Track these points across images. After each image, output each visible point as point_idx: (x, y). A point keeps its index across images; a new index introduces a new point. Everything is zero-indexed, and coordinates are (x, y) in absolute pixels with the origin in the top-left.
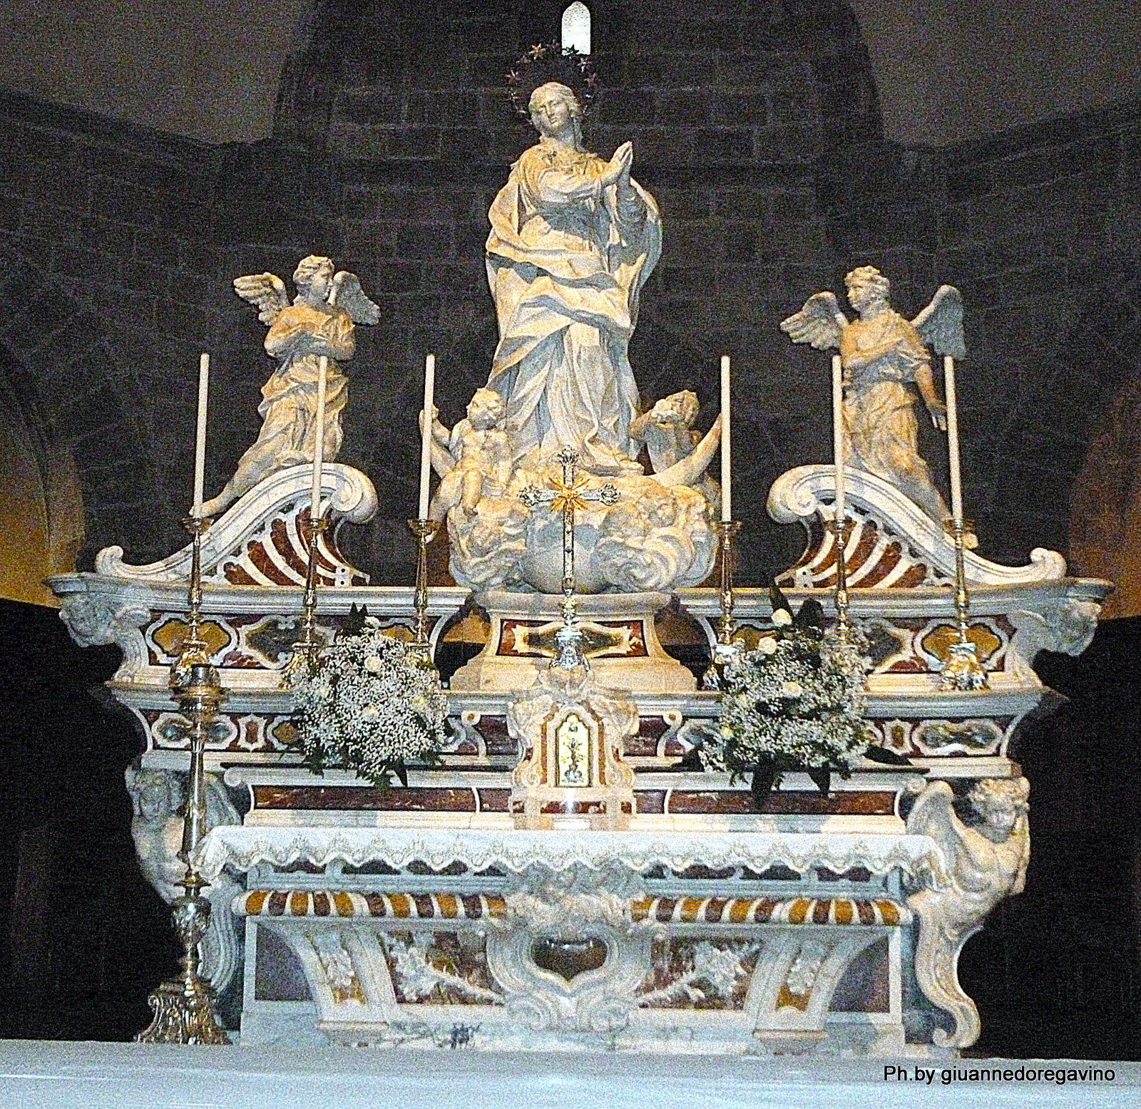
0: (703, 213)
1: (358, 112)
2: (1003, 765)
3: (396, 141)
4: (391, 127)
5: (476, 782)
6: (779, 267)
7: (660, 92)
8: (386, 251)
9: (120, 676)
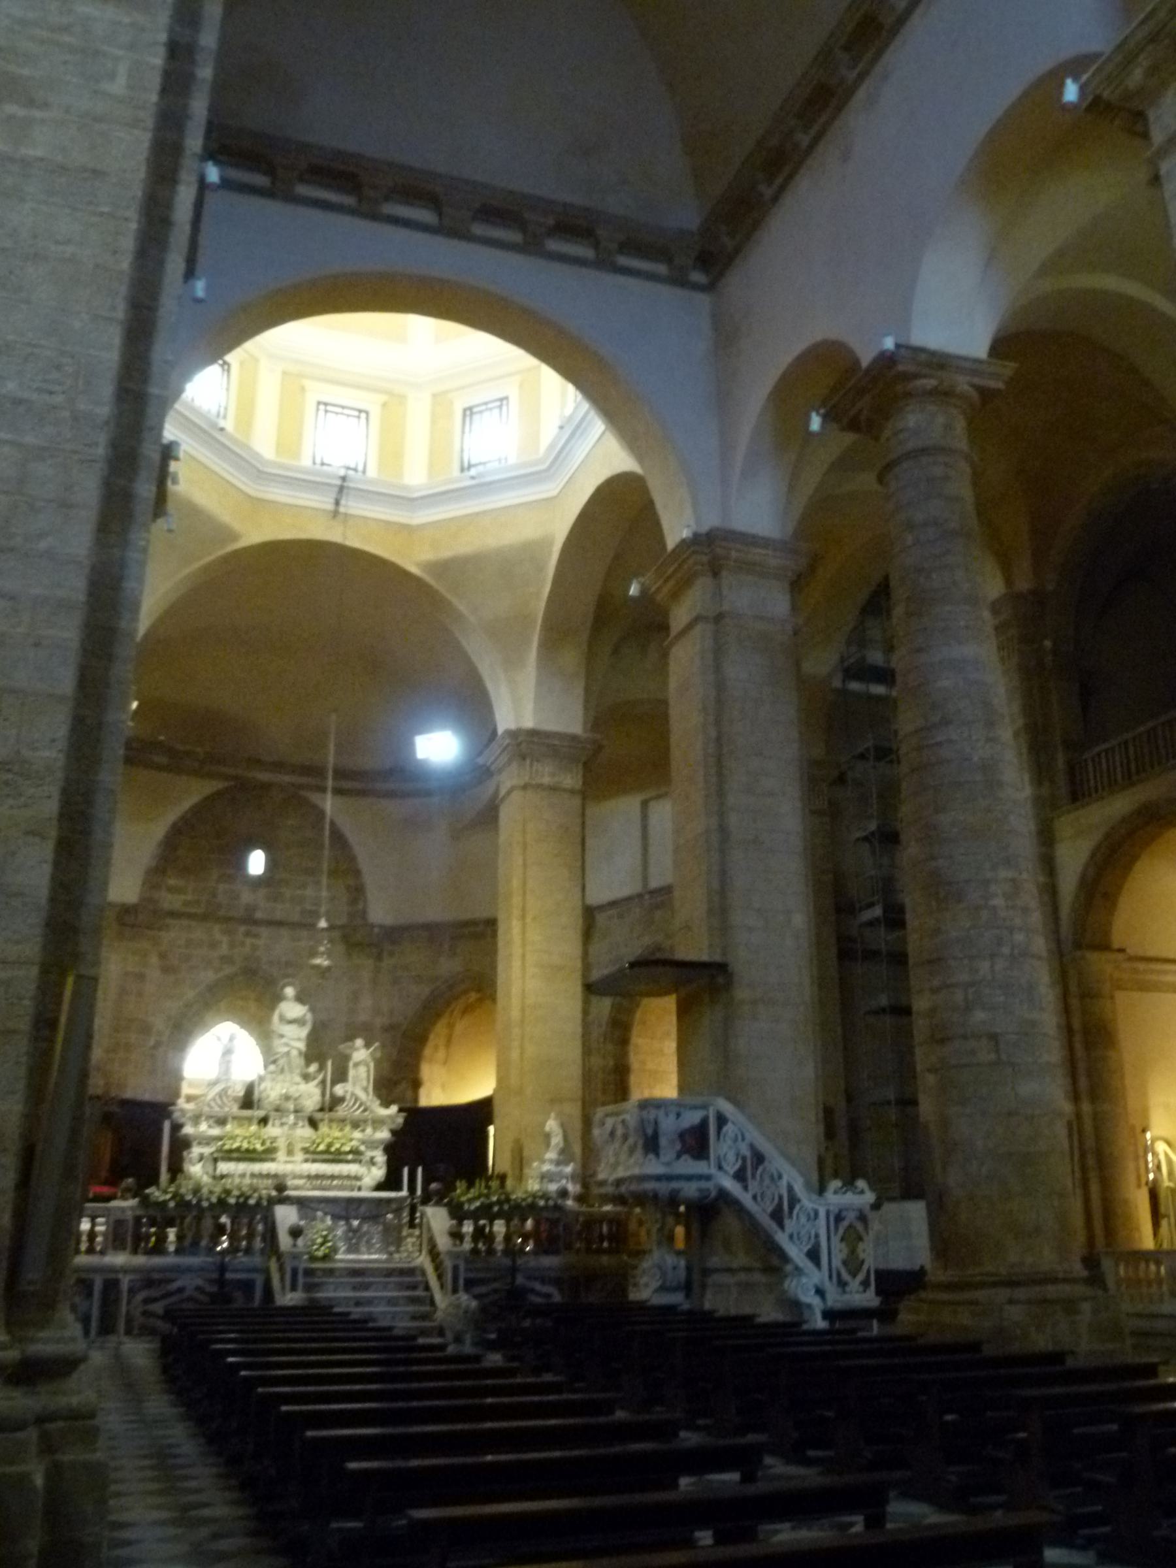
1: (170, 890)
3: (186, 904)
4: (183, 897)
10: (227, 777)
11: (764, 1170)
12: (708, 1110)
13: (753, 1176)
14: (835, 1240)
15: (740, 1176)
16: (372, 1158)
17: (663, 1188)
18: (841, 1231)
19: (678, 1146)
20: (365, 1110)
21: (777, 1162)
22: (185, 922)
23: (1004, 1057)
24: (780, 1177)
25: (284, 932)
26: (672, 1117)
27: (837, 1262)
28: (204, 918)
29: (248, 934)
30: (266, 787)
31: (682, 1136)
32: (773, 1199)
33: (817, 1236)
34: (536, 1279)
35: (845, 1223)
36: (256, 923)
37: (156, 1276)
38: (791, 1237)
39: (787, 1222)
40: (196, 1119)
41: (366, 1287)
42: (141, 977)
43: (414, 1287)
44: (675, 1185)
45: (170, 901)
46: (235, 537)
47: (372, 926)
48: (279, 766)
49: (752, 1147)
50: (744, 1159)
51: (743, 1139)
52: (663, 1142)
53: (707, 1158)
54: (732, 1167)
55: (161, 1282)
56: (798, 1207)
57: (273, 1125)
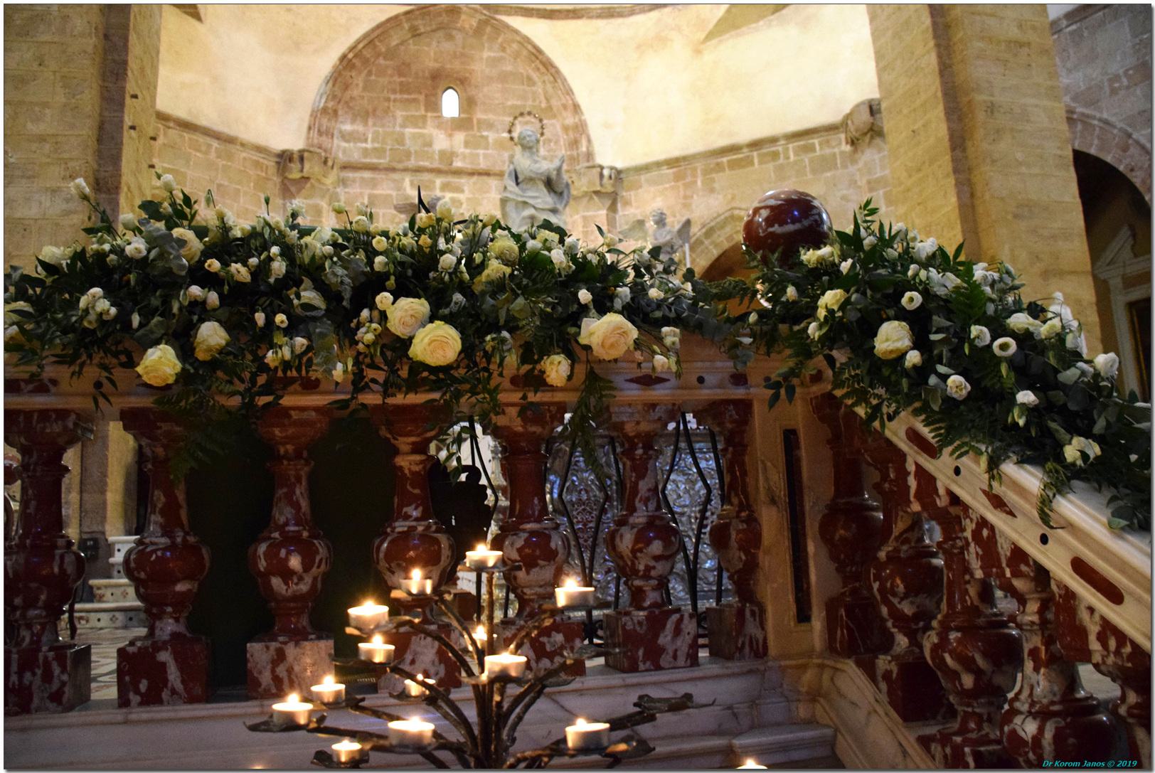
1: (345, 137)
3: (366, 152)
4: (364, 145)
22: (367, 175)
29: (445, 187)
36: (458, 173)
45: (342, 149)
47: (602, 168)
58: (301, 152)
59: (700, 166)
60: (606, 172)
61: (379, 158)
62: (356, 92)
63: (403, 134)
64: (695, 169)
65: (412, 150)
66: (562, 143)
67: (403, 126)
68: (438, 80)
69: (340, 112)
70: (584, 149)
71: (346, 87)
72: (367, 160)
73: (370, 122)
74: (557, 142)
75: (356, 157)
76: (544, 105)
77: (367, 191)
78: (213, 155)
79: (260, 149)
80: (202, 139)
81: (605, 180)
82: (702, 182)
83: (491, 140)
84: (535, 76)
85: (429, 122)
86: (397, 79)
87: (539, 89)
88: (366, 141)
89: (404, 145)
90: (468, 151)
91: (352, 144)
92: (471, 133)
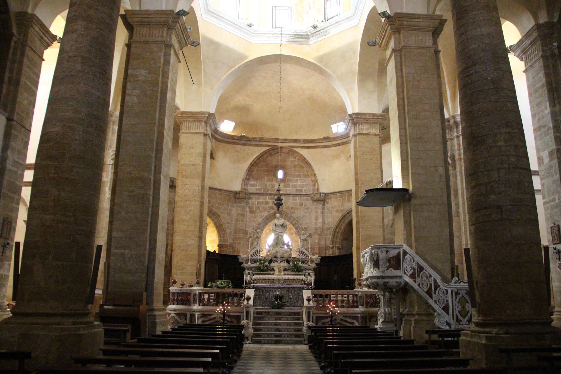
0: (296, 200)
1: (251, 185)
2: (312, 272)
3: (257, 190)
4: (256, 188)
5: (272, 273)
6: (306, 207)
7: (291, 184)
8: (256, 204)
9: (243, 265)
10: (268, 146)
11: (423, 273)
12: (400, 249)
13: (419, 276)
14: (456, 302)
15: (412, 276)
16: (309, 273)
17: (380, 281)
18: (457, 300)
19: (388, 265)
20: (306, 257)
21: (428, 270)
23: (505, 217)
24: (431, 276)
25: (291, 197)
26: (384, 253)
27: (456, 312)
28: (263, 194)
30: (281, 148)
31: (389, 260)
32: (427, 286)
33: (447, 301)
34: (347, 317)
35: (460, 296)
37: (206, 313)
38: (435, 301)
39: (433, 295)
40: (247, 261)
41: (280, 319)
42: (243, 215)
43: (298, 319)
44: (386, 280)
45: (251, 189)
46: (246, 57)
47: (321, 193)
48: (285, 140)
49: (418, 264)
50: (414, 269)
51: (414, 261)
52: (381, 263)
53: (400, 269)
54: (409, 272)
55: (207, 315)
56: (438, 289)
57: (274, 262)
58: (240, 191)
59: (347, 194)
60: (322, 195)
61: (260, 191)
62: (254, 173)
63: (267, 184)
64: (345, 195)
65: (269, 188)
66: (311, 185)
67: (267, 182)
68: (276, 168)
69: (250, 178)
70: (316, 187)
71: (252, 171)
72: (257, 192)
73: (258, 181)
74: (310, 185)
75: (254, 191)
76: (306, 174)
77: (257, 201)
78: (217, 195)
79: (229, 191)
80: (214, 191)
81: (321, 197)
82: (347, 199)
83: (291, 185)
84: (304, 165)
85: (274, 181)
86: (266, 168)
87: (305, 169)
88: (257, 186)
89: (266, 187)
90: (284, 188)
91: (253, 188)
92: (285, 183)
